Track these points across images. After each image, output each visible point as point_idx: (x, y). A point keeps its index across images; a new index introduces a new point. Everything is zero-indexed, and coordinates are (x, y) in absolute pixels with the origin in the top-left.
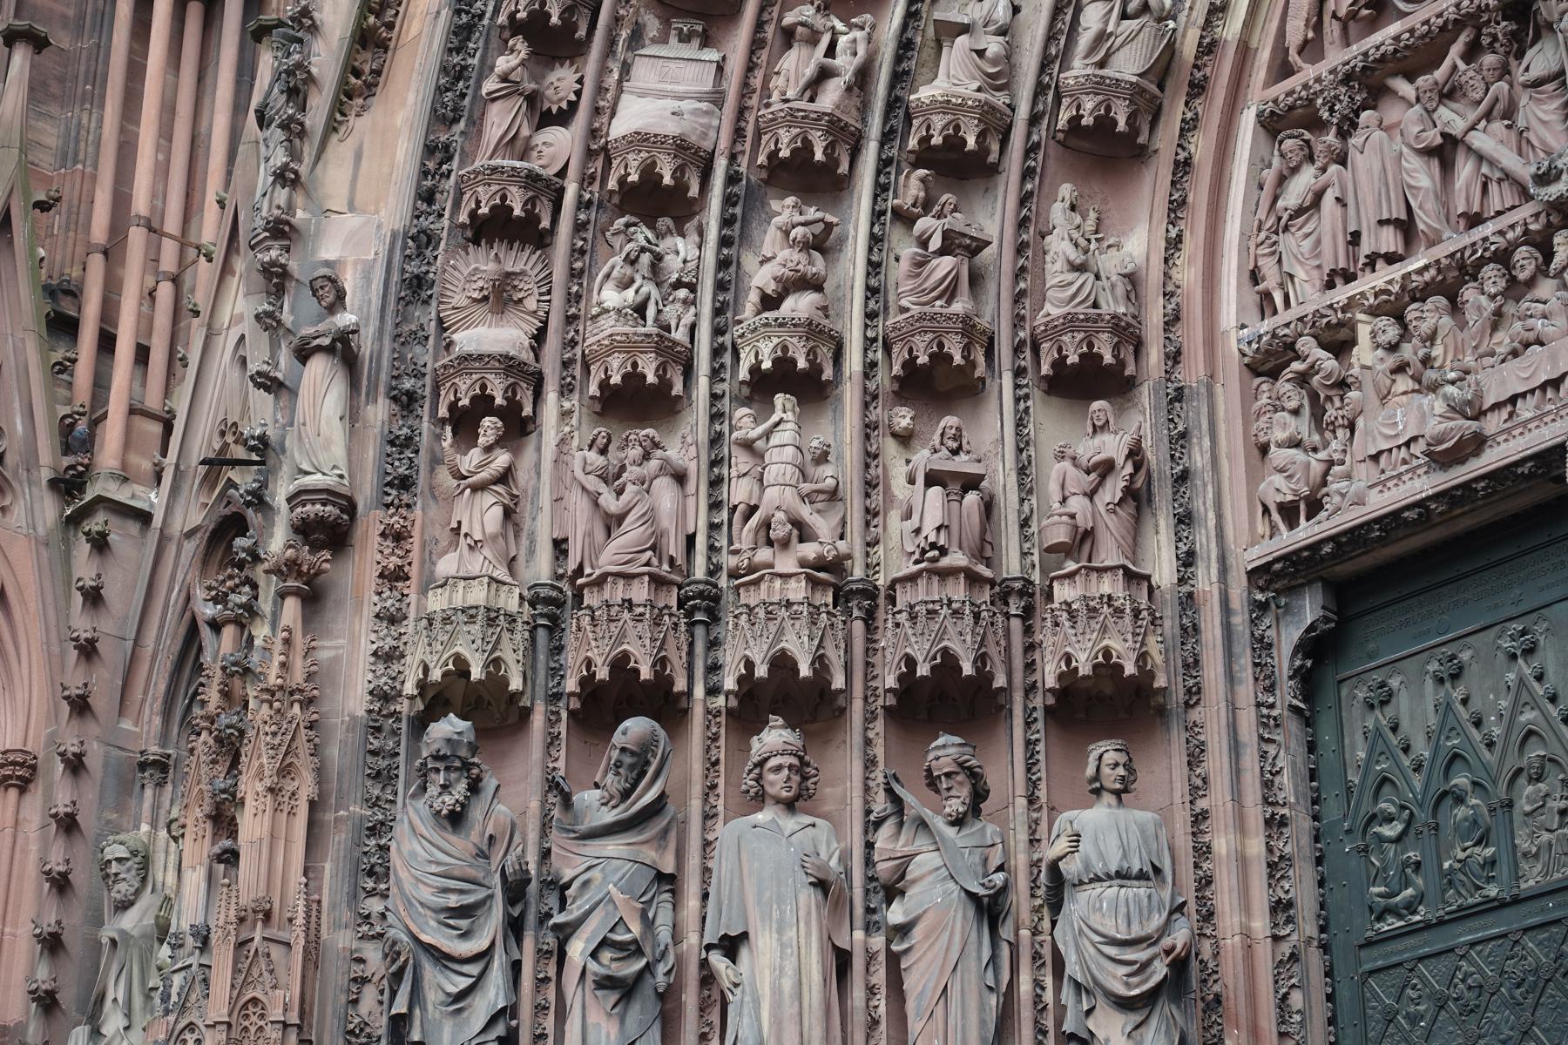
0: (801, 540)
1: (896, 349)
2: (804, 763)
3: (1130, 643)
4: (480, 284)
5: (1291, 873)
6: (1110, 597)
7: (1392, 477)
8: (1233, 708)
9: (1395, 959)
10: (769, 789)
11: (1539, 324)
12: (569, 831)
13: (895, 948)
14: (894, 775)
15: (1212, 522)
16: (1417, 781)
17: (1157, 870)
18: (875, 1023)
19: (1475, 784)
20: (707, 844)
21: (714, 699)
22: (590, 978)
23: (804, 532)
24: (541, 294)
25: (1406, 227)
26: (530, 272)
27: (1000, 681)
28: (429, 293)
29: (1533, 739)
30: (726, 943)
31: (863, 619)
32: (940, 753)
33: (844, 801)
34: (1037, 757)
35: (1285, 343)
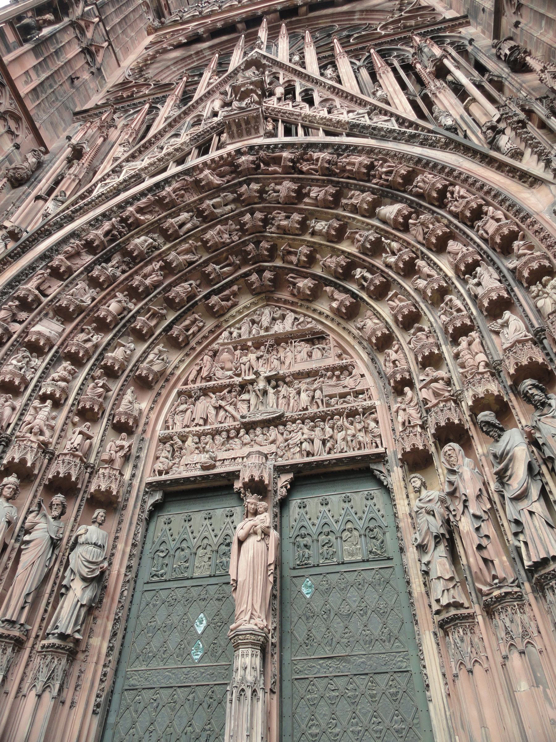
0: (40, 435)
2: (17, 489)
10: (4, 493)
11: (234, 446)
13: (23, 547)
15: (141, 469)
17: (104, 547)
23: (41, 433)
25: (206, 421)
27: (79, 486)
33: (23, 504)
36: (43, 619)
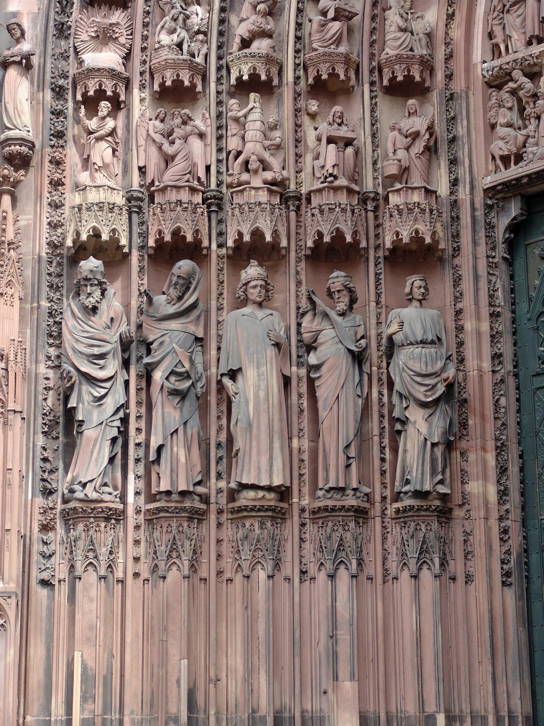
0: (264, 170)
1: (310, 70)
3: (428, 227)
4: (95, 29)
5: (501, 340)
6: (419, 203)
8: (475, 258)
10: (250, 297)
12: (152, 317)
13: (313, 376)
14: (312, 291)
15: (467, 164)
17: (439, 339)
18: (302, 411)
20: (219, 322)
21: (220, 250)
22: (165, 390)
24: (127, 35)
26: (122, 23)
27: (363, 244)
28: (69, 32)
30: (231, 373)
32: (335, 280)
34: (380, 281)
35: (506, 73)
36: (383, 473)
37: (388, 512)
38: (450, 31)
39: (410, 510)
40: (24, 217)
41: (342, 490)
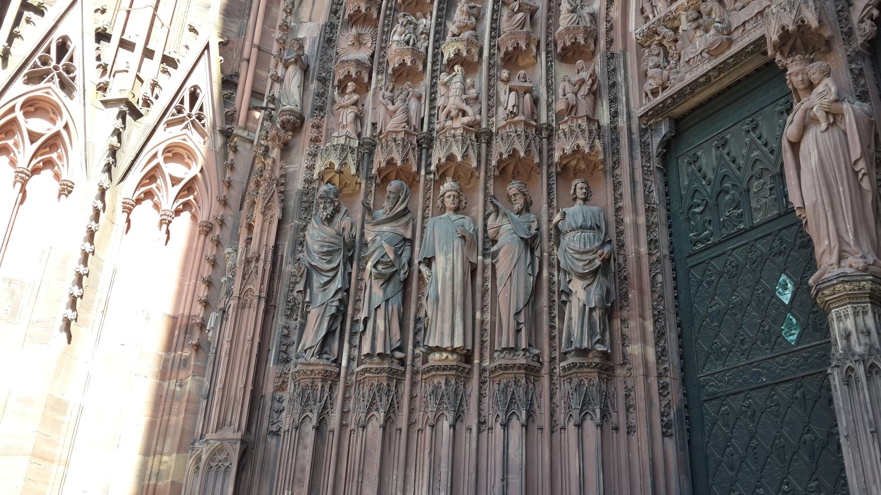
4: (351, 39)
5: (657, 229)
7: (694, 67)
8: (632, 168)
9: (701, 260)
10: (447, 205)
16: (709, 189)
17: (599, 227)
18: (487, 290)
19: (733, 185)
23: (464, 114)
29: (758, 162)
31: (485, 143)
36: (552, 338)
37: (557, 371)
38: (610, 13)
39: (573, 367)
40: (292, 166)
41: (513, 350)
